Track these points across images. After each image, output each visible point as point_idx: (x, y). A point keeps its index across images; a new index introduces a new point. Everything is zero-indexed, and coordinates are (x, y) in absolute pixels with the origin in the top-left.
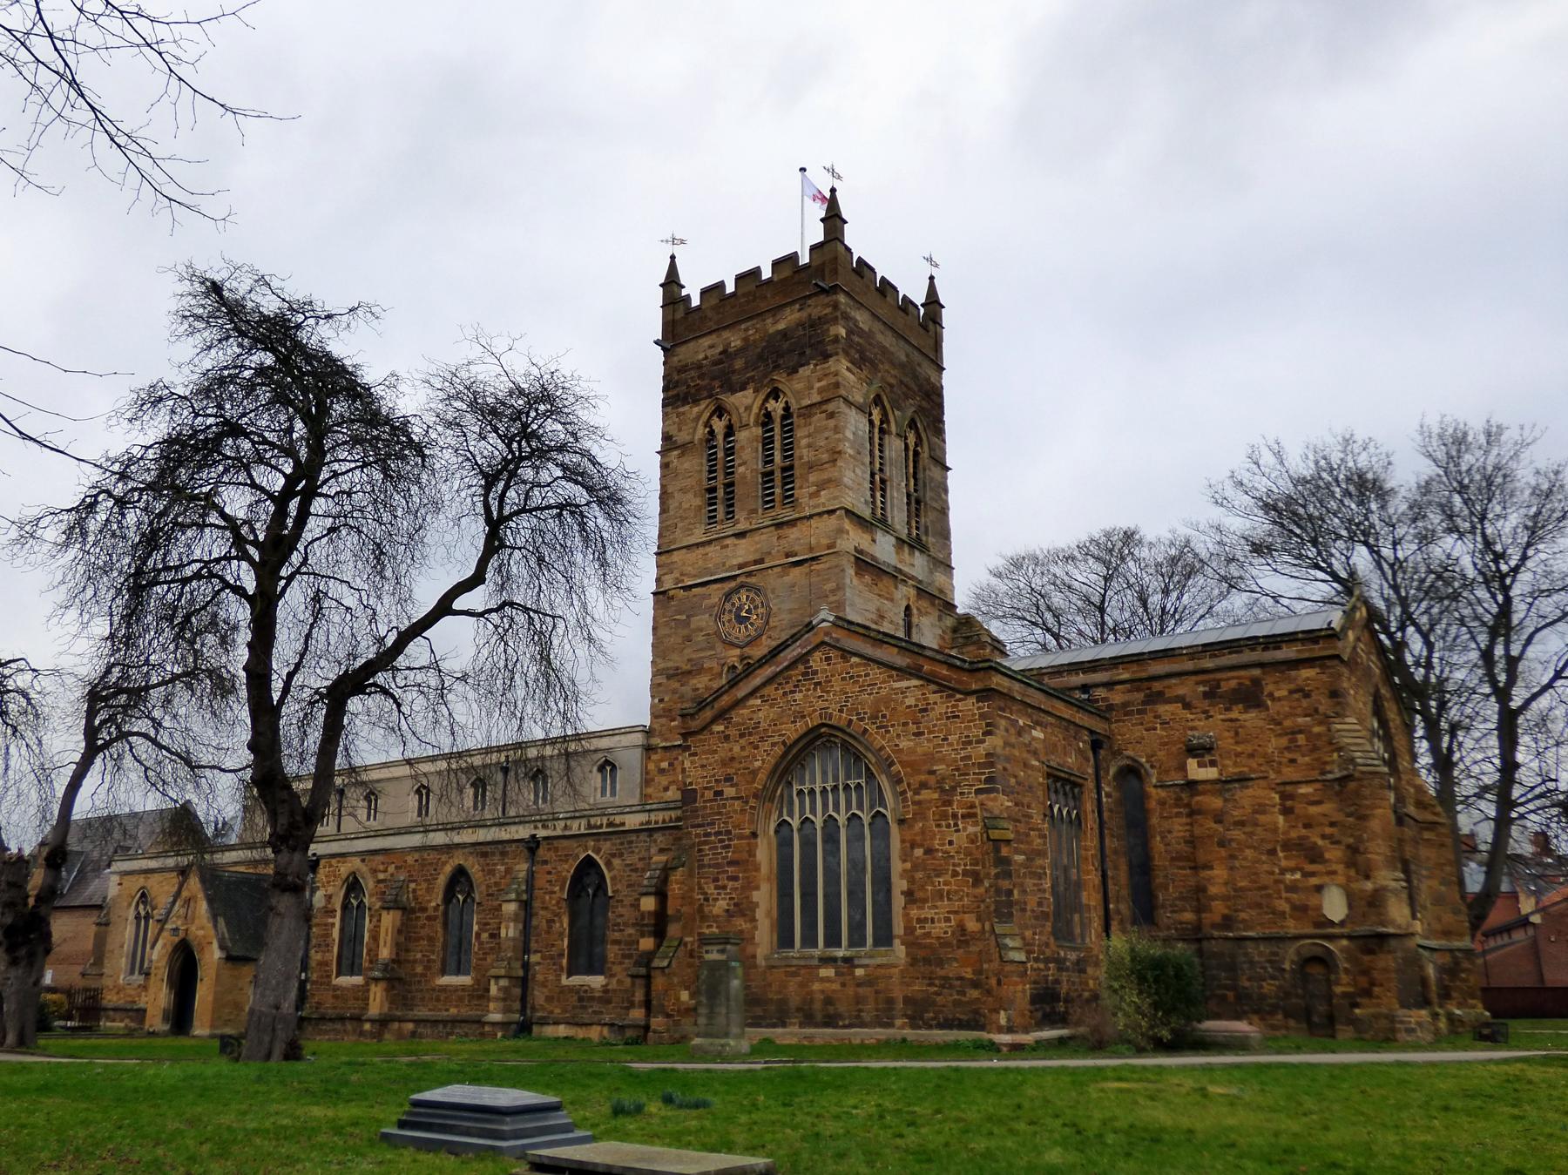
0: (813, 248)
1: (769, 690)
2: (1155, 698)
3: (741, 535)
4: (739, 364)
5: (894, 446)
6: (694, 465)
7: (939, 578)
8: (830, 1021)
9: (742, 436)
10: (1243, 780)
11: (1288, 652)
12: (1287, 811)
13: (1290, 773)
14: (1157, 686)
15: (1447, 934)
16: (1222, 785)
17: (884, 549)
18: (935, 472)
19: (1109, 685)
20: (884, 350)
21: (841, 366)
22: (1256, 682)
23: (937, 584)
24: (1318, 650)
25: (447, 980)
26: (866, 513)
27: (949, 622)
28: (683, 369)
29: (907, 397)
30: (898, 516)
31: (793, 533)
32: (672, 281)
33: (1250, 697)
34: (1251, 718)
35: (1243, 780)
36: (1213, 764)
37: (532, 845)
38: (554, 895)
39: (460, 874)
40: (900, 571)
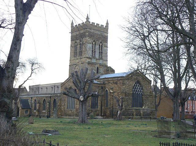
0: (85, 22)
1: (67, 82)
2: (109, 83)
3: (77, 59)
4: (78, 36)
5: (97, 47)
6: (73, 49)
7: (104, 62)
8: (70, 116)
9: (78, 46)
10: (115, 92)
11: (119, 79)
12: (118, 96)
13: (119, 92)
14: (109, 81)
15: (152, 108)
16: (113, 93)
17: (94, 61)
18: (105, 48)
19: (106, 81)
20: (95, 34)
21: (87, 38)
22: (117, 82)
23: (104, 63)
24: (122, 78)
25: (44, 111)
26: (91, 57)
27: (105, 68)
28: (73, 36)
29: (100, 39)
30: (97, 56)
31: (82, 59)
32: (72, 24)
33: (116, 83)
34: (116, 85)
35: (115, 92)
36: (113, 90)
37: (50, 97)
38: (52, 102)
39: (44, 100)
40: (97, 63)
